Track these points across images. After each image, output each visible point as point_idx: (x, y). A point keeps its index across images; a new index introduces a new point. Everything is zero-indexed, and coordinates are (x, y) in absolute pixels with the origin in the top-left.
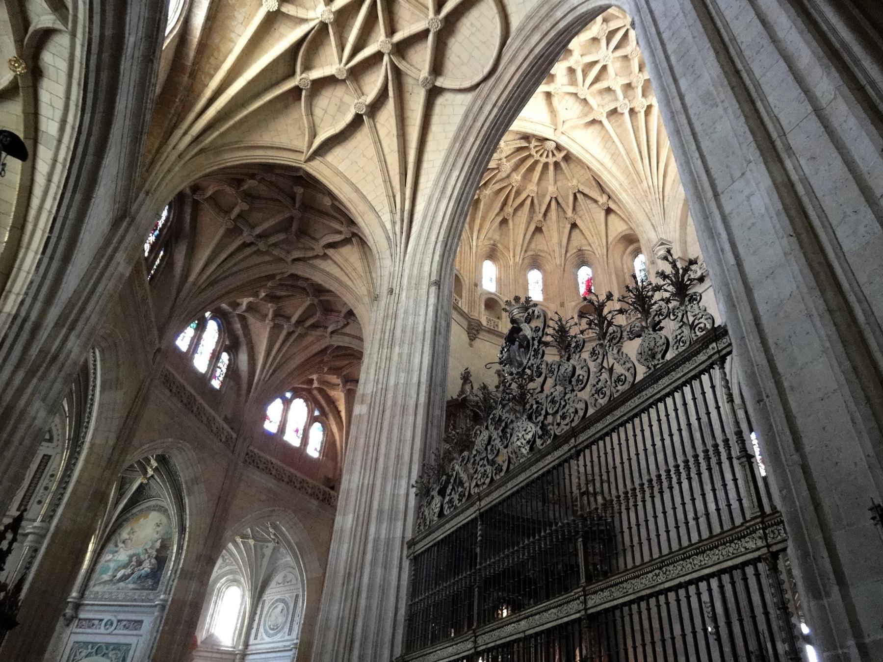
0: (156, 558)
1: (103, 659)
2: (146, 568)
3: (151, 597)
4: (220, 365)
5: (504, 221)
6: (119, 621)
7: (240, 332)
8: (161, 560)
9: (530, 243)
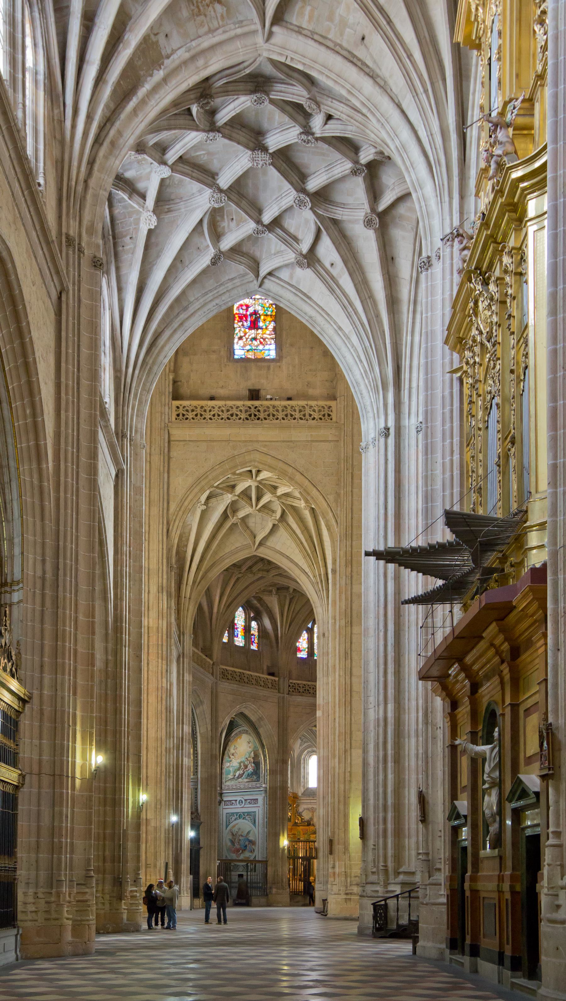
0: (254, 763)
1: (244, 821)
2: (250, 769)
3: (258, 785)
4: (252, 632)
6: (245, 800)
7: (258, 605)
8: (257, 764)
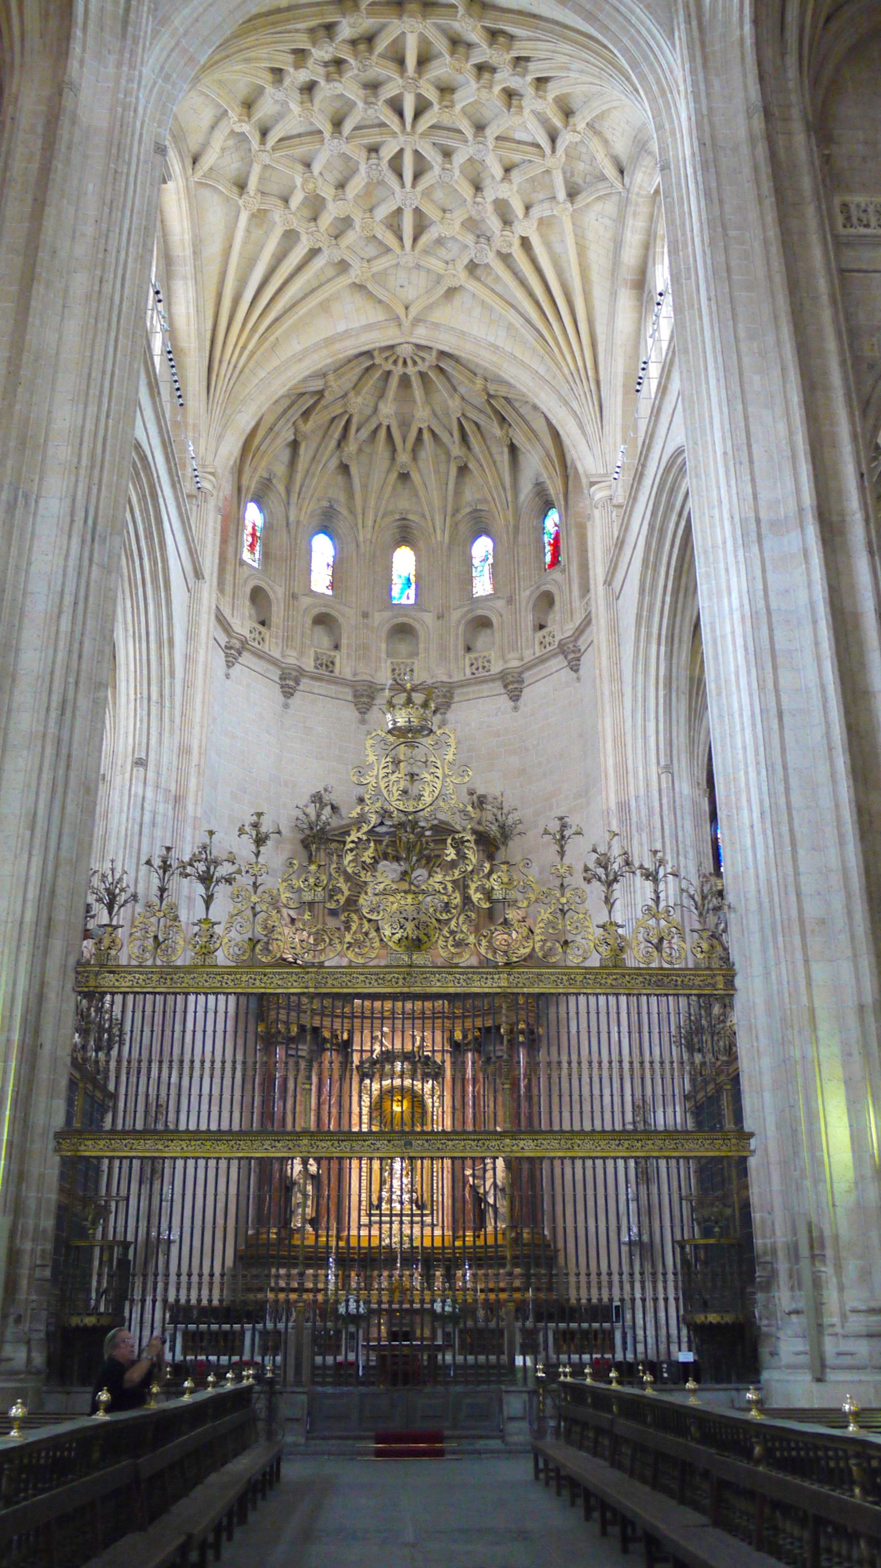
5: (404, 477)
9: (458, 493)
